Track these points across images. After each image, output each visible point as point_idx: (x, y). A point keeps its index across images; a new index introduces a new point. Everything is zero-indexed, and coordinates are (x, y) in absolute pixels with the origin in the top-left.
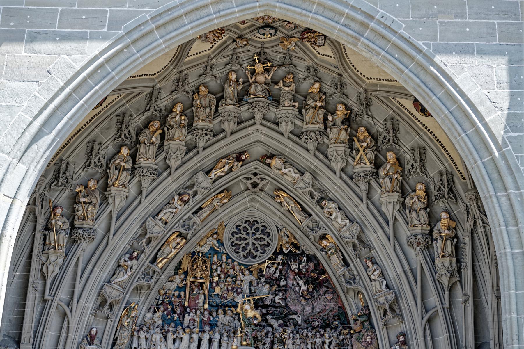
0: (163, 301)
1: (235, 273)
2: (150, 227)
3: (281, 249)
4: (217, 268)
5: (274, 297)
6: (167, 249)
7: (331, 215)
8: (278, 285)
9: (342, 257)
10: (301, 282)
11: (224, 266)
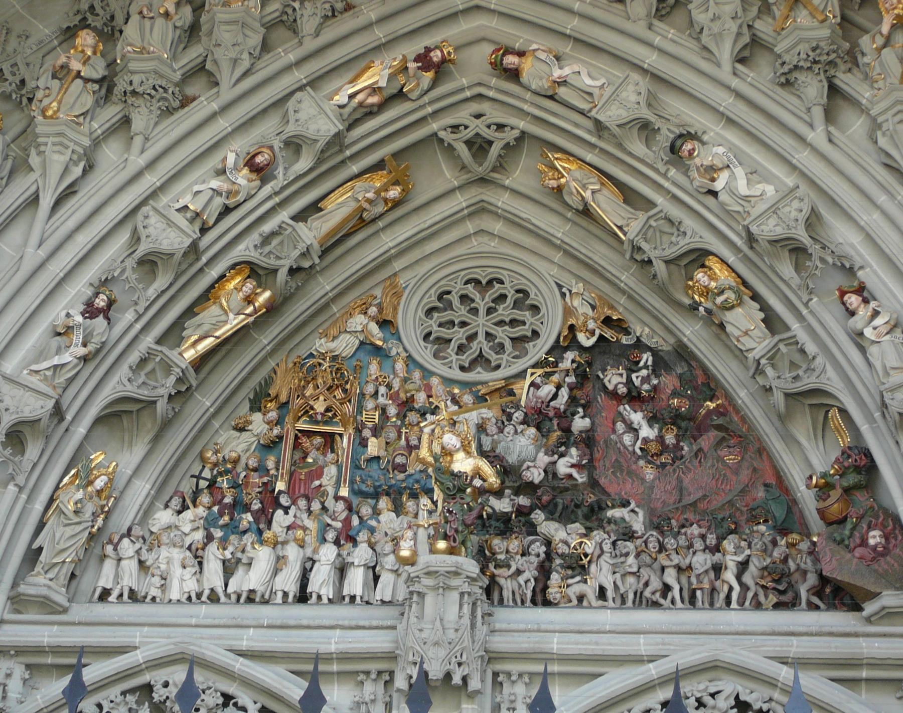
0: (212, 484)
1: (431, 403)
2: (151, 230)
3: (574, 339)
4: (376, 393)
5: (555, 463)
6: (211, 312)
7: (713, 180)
8: (567, 431)
9: (762, 315)
10: (637, 418)
11: (396, 385)
